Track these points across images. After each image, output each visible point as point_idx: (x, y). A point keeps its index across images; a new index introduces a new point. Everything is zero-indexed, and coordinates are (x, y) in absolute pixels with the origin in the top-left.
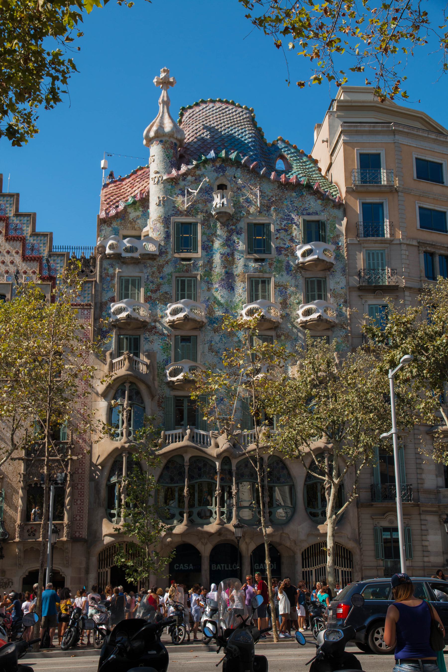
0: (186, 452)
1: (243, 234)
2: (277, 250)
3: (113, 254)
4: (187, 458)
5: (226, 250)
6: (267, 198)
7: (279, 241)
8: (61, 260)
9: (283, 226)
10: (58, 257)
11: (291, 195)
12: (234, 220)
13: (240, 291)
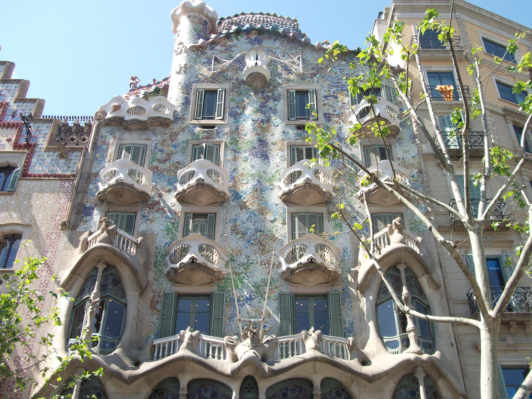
0: (183, 371)
1: (282, 101)
2: (325, 117)
3: (113, 117)
4: (184, 380)
5: (259, 116)
6: (310, 66)
7: (327, 107)
8: (47, 127)
9: (331, 93)
10: (44, 123)
11: (340, 64)
12: (271, 87)
13: (278, 160)
